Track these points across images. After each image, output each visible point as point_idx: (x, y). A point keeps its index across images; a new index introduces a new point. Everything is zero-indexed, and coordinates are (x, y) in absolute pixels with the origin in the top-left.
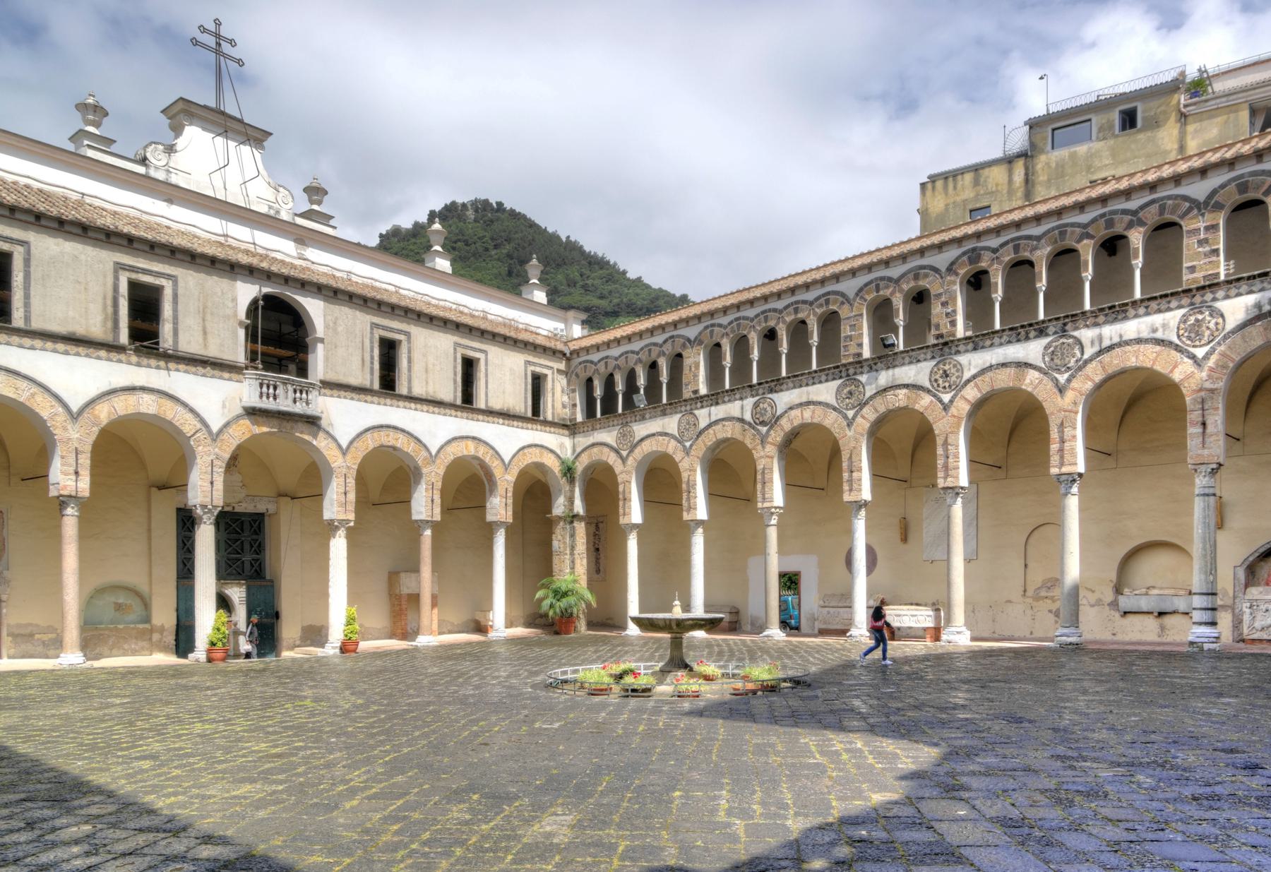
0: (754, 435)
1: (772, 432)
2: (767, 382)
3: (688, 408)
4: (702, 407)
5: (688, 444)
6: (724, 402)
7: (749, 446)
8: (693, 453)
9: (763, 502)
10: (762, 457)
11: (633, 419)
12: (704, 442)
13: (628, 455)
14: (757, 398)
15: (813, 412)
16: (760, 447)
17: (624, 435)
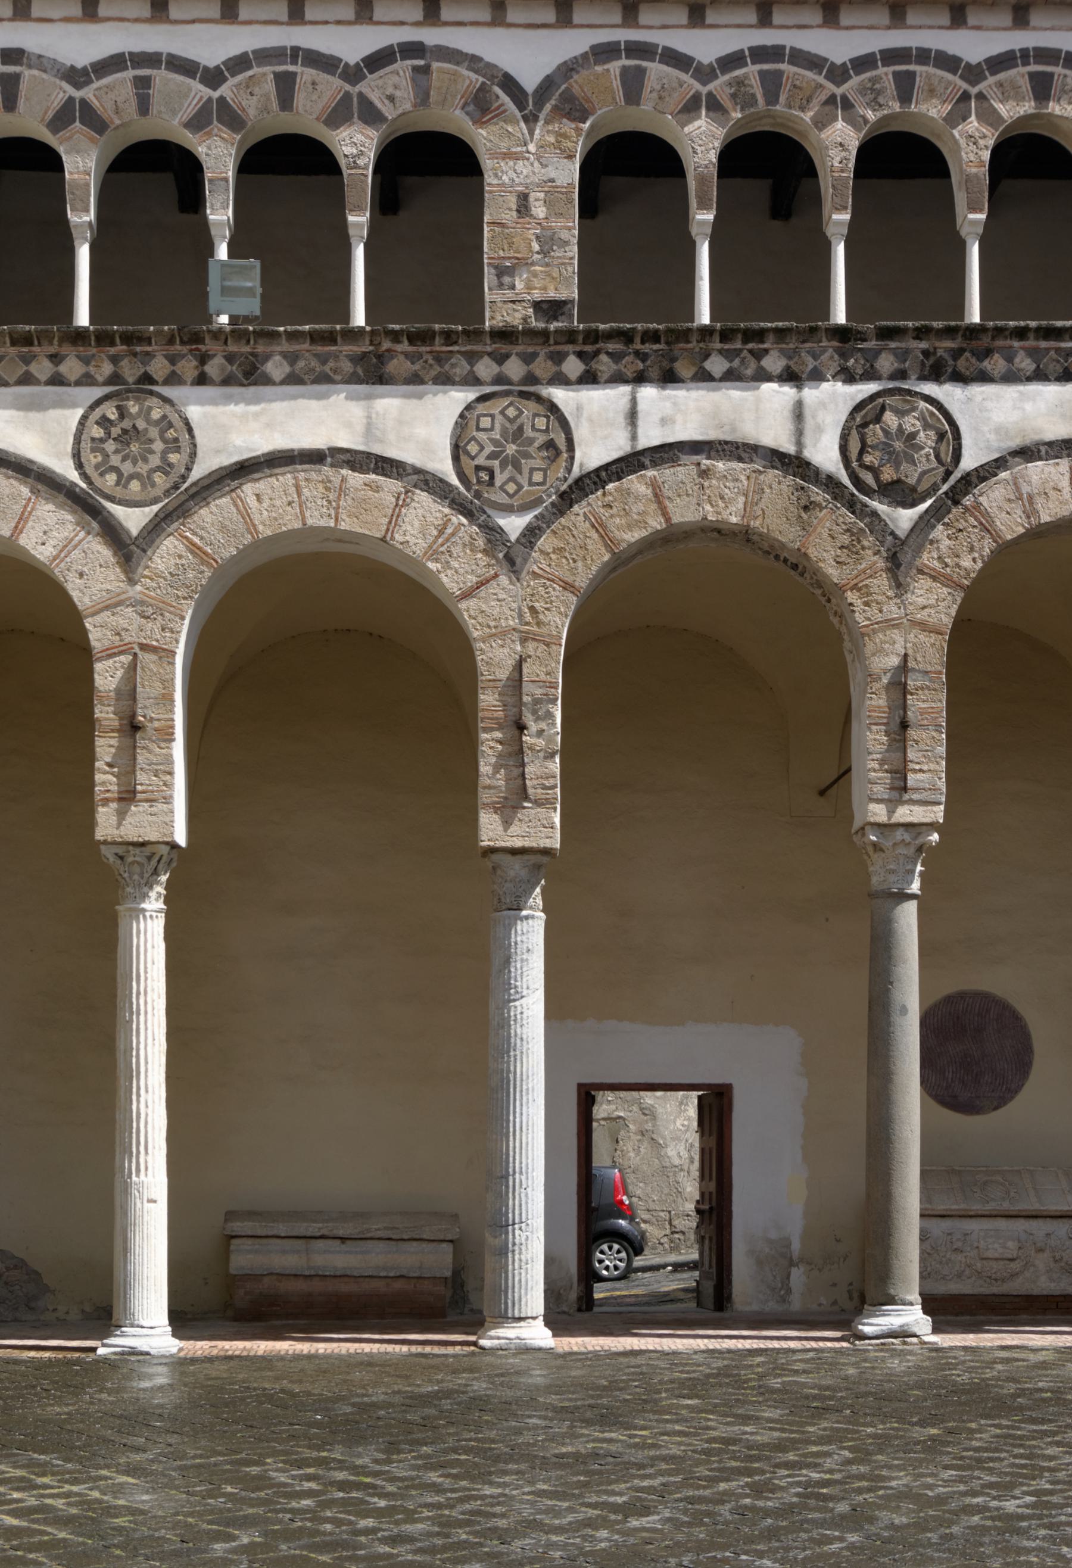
0: (856, 535)
1: (939, 532)
2: (921, 333)
3: (514, 368)
4: (590, 379)
5: (514, 525)
6: (704, 377)
7: (832, 572)
8: (537, 562)
9: (892, 804)
10: (891, 624)
11: (188, 367)
12: (599, 527)
14: (870, 388)
16: (881, 583)
17: (127, 436)
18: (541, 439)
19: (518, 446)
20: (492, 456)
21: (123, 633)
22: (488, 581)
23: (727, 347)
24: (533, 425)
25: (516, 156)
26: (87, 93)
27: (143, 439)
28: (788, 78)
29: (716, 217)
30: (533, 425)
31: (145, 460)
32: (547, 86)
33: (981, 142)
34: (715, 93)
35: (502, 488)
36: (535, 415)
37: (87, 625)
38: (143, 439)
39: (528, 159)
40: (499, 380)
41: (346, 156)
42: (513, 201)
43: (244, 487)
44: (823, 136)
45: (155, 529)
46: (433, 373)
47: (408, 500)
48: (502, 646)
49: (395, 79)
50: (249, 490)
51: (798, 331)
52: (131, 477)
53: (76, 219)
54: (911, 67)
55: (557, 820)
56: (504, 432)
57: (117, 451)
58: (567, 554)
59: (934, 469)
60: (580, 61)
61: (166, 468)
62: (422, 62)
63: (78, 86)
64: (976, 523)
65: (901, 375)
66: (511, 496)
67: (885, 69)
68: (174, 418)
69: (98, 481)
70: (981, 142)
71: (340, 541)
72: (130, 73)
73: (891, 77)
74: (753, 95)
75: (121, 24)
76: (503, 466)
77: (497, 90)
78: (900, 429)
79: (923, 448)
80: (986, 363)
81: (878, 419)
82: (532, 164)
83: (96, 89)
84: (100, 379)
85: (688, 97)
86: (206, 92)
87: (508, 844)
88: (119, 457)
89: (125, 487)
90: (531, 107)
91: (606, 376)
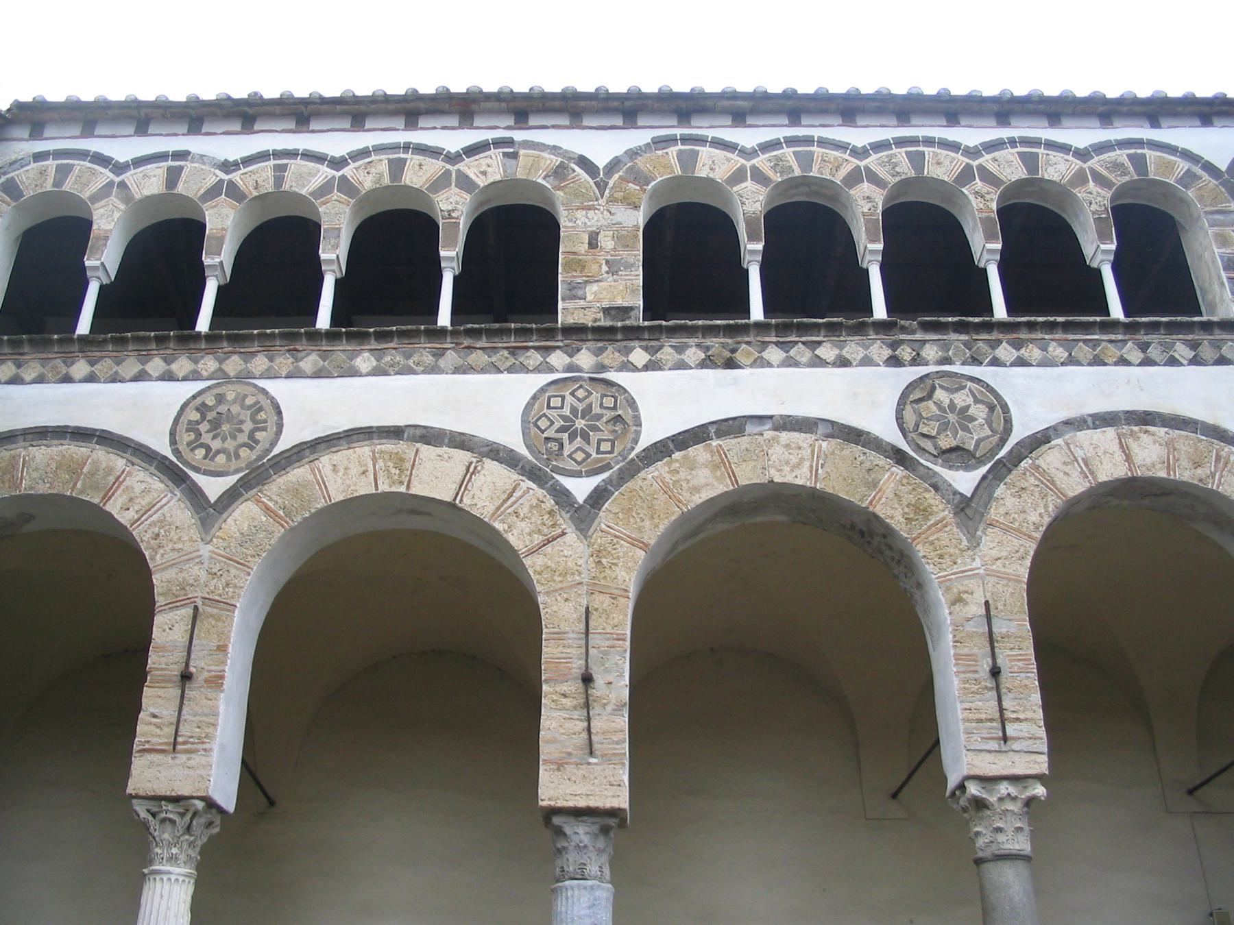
1: (1000, 490)
5: (580, 488)
13: (231, 497)
15: (1170, 445)
18: (609, 415)
19: (586, 421)
20: (562, 429)
21: (187, 588)
22: (554, 539)
23: (781, 340)
24: (601, 404)
25: (589, 208)
26: (236, 177)
27: (235, 421)
28: (818, 157)
29: (764, 247)
30: (601, 404)
31: (234, 437)
32: (614, 165)
33: (988, 197)
34: (757, 165)
35: (570, 456)
36: (603, 396)
37: (154, 581)
38: (235, 421)
39: (599, 210)
40: (571, 368)
41: (442, 211)
42: (586, 238)
43: (321, 459)
44: (851, 192)
45: (231, 497)
46: (508, 364)
47: (479, 468)
48: (567, 600)
49: (488, 161)
50: (325, 461)
51: (847, 327)
52: (218, 452)
53: (209, 260)
54: (921, 149)
55: (626, 778)
56: (574, 410)
57: (208, 432)
58: (634, 514)
59: (988, 437)
60: (643, 149)
61: (252, 442)
62: (512, 150)
63: (227, 173)
64: (1037, 483)
65: (946, 361)
66: (579, 463)
67: (899, 150)
68: (266, 403)
69: (187, 455)
70: (988, 197)
71: (413, 512)
72: (272, 162)
73: (904, 154)
74: (791, 167)
75: (271, 134)
76: (572, 438)
77: (573, 166)
78: (952, 406)
79: (976, 419)
80: (1023, 351)
81: (930, 396)
82: (602, 213)
83: (242, 174)
84: (205, 374)
85: (735, 168)
86: (331, 172)
87: (570, 804)
88: (211, 435)
89: (212, 459)
90: (601, 176)
91: (670, 364)
